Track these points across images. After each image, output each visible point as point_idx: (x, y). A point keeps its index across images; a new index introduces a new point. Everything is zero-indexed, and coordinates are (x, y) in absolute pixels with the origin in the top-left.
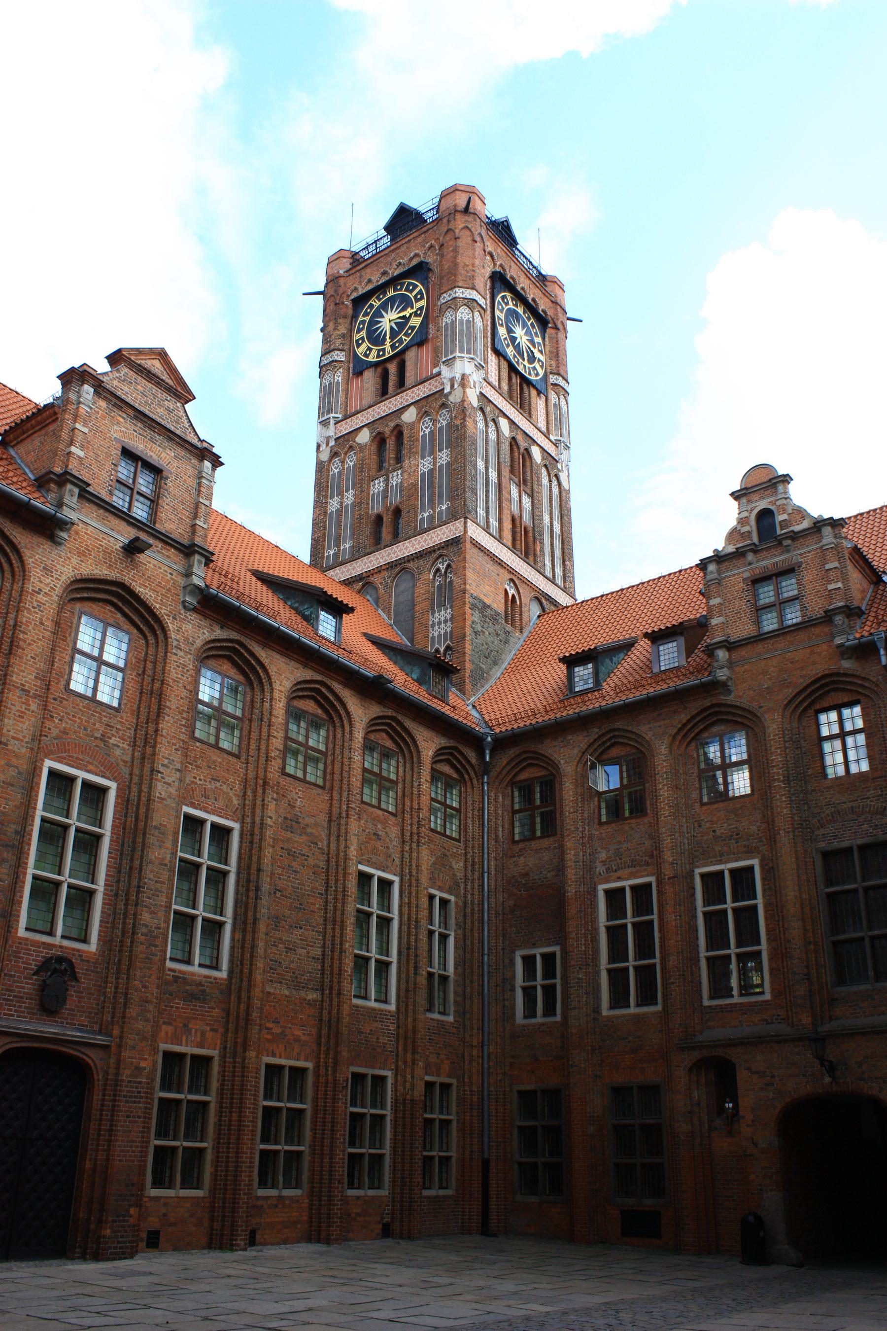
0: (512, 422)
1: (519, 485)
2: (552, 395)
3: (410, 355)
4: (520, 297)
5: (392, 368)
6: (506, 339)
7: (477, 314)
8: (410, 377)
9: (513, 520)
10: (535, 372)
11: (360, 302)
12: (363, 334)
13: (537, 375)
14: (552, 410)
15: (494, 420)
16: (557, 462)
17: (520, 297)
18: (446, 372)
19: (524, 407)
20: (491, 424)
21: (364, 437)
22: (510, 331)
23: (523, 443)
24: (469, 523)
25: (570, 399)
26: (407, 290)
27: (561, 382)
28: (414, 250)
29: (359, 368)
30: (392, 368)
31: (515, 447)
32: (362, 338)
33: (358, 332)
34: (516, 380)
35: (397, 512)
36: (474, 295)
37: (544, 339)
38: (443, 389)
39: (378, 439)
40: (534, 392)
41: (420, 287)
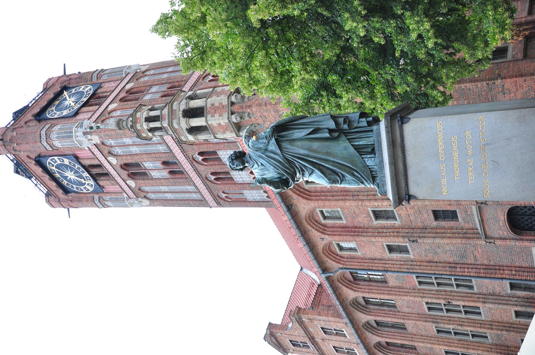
1: (145, 95)
4: (50, 103)
5: (95, 171)
6: (70, 110)
7: (54, 129)
8: (96, 162)
9: (162, 97)
11: (66, 191)
13: (90, 89)
15: (109, 113)
16: (136, 72)
17: (50, 103)
20: (112, 115)
22: (66, 108)
25: (105, 68)
27: (96, 73)
29: (99, 190)
30: (95, 171)
31: (124, 99)
32: (85, 188)
33: (81, 190)
34: (93, 101)
35: (165, 163)
36: (43, 132)
37: (73, 88)
38: (95, 144)
39: (131, 176)
40: (99, 91)
41: (49, 160)
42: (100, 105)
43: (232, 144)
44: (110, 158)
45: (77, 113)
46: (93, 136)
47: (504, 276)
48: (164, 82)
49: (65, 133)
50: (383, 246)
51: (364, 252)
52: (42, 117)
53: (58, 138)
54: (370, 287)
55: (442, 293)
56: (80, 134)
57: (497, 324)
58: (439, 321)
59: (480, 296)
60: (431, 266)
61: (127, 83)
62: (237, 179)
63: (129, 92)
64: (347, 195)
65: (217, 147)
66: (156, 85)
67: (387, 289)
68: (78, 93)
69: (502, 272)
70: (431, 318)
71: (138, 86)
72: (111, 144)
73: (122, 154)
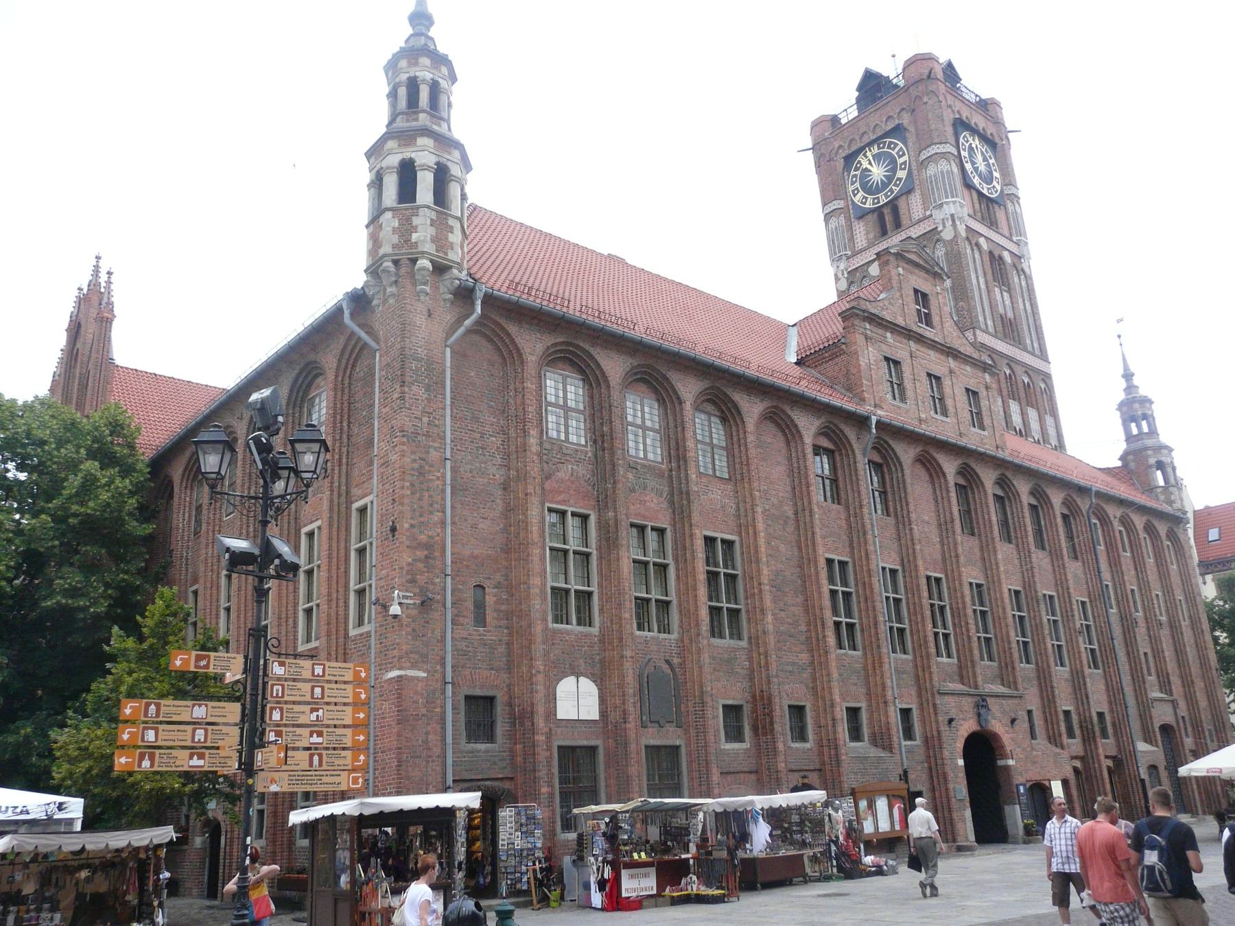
2: (1009, 205)
3: (902, 204)
8: (905, 221)
10: (993, 190)
12: (857, 185)
17: (974, 131)
18: (938, 215)
19: (992, 224)
22: (973, 163)
23: (996, 254)
24: (978, 332)
25: (1021, 201)
26: (889, 147)
28: (887, 113)
29: (862, 215)
40: (996, 207)
42: (982, 221)
45: (969, 186)
52: (960, 129)
56: (949, 209)
63: (1001, 258)
68: (991, 173)
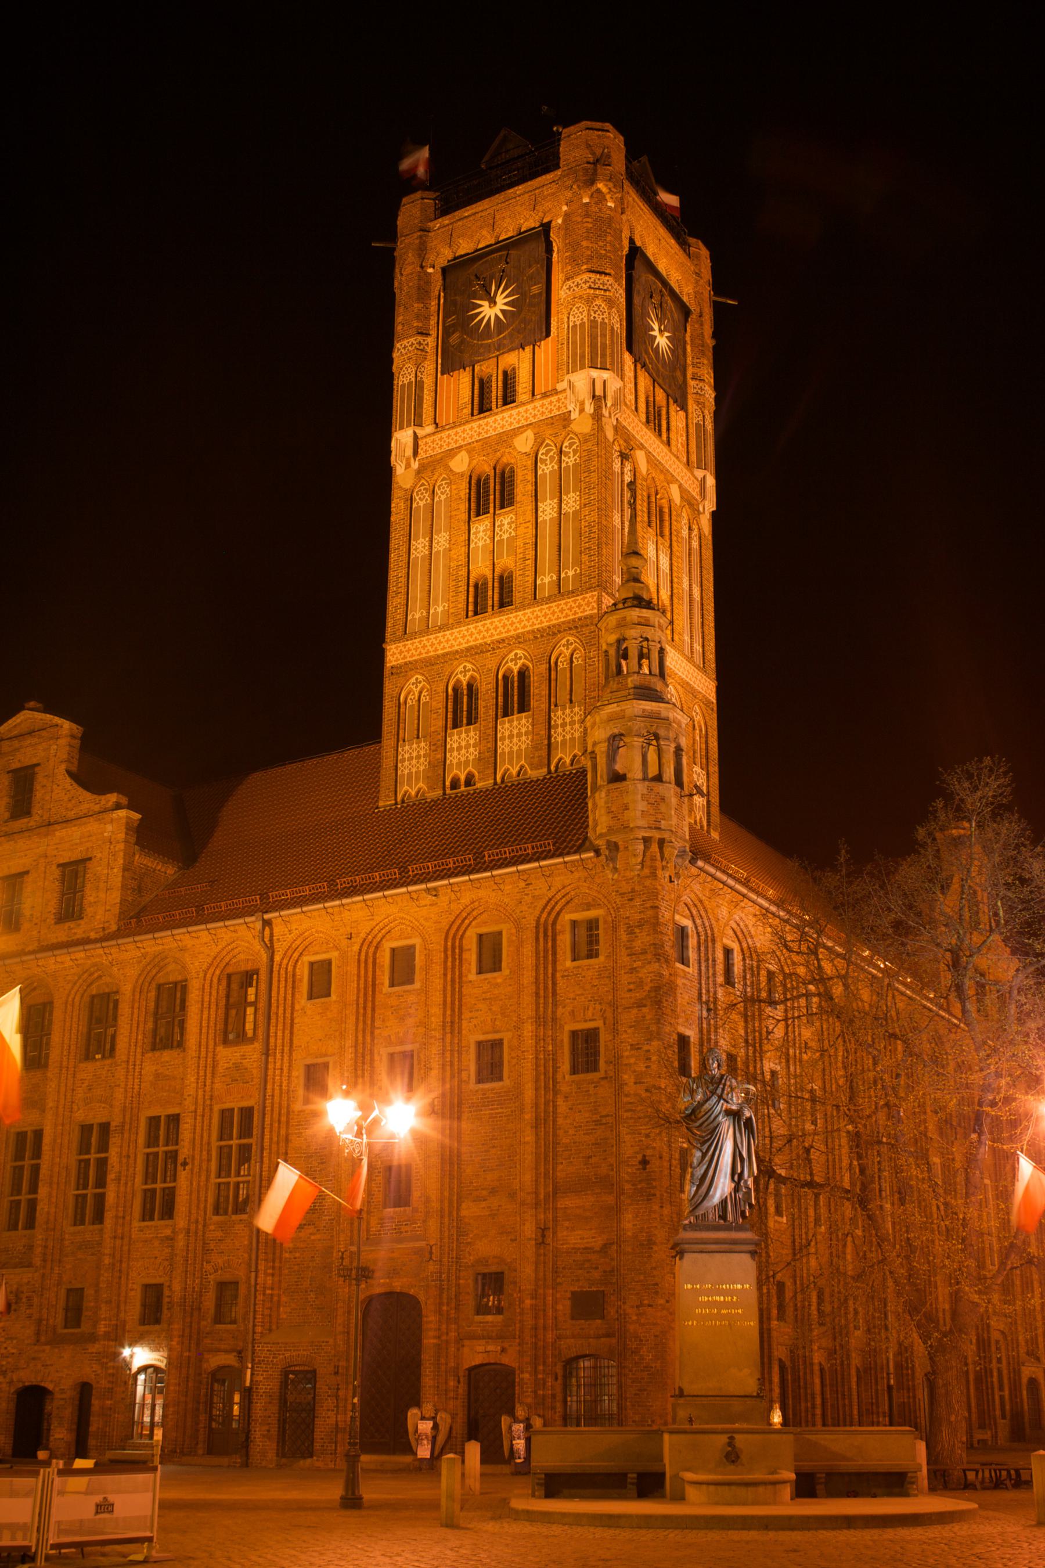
0: (648, 454)
14: (692, 430)
21: (460, 464)
43: (544, 753)
44: (529, 434)
46: (590, 421)
47: (261, 1275)
48: (675, 586)
49: (604, 345)
50: (326, 1055)
51: (309, 1012)
53: (593, 323)
54: (213, 1007)
55: (205, 1153)
57: (126, 1248)
58: (126, 1135)
59: (200, 1227)
60: (278, 1143)
61: (680, 486)
62: (456, 737)
64: (453, 1010)
65: (542, 718)
66: (671, 565)
67: (211, 1043)
69: (270, 1271)
70: (131, 1119)
71: (674, 518)
72: (567, 454)
73: (540, 472)
